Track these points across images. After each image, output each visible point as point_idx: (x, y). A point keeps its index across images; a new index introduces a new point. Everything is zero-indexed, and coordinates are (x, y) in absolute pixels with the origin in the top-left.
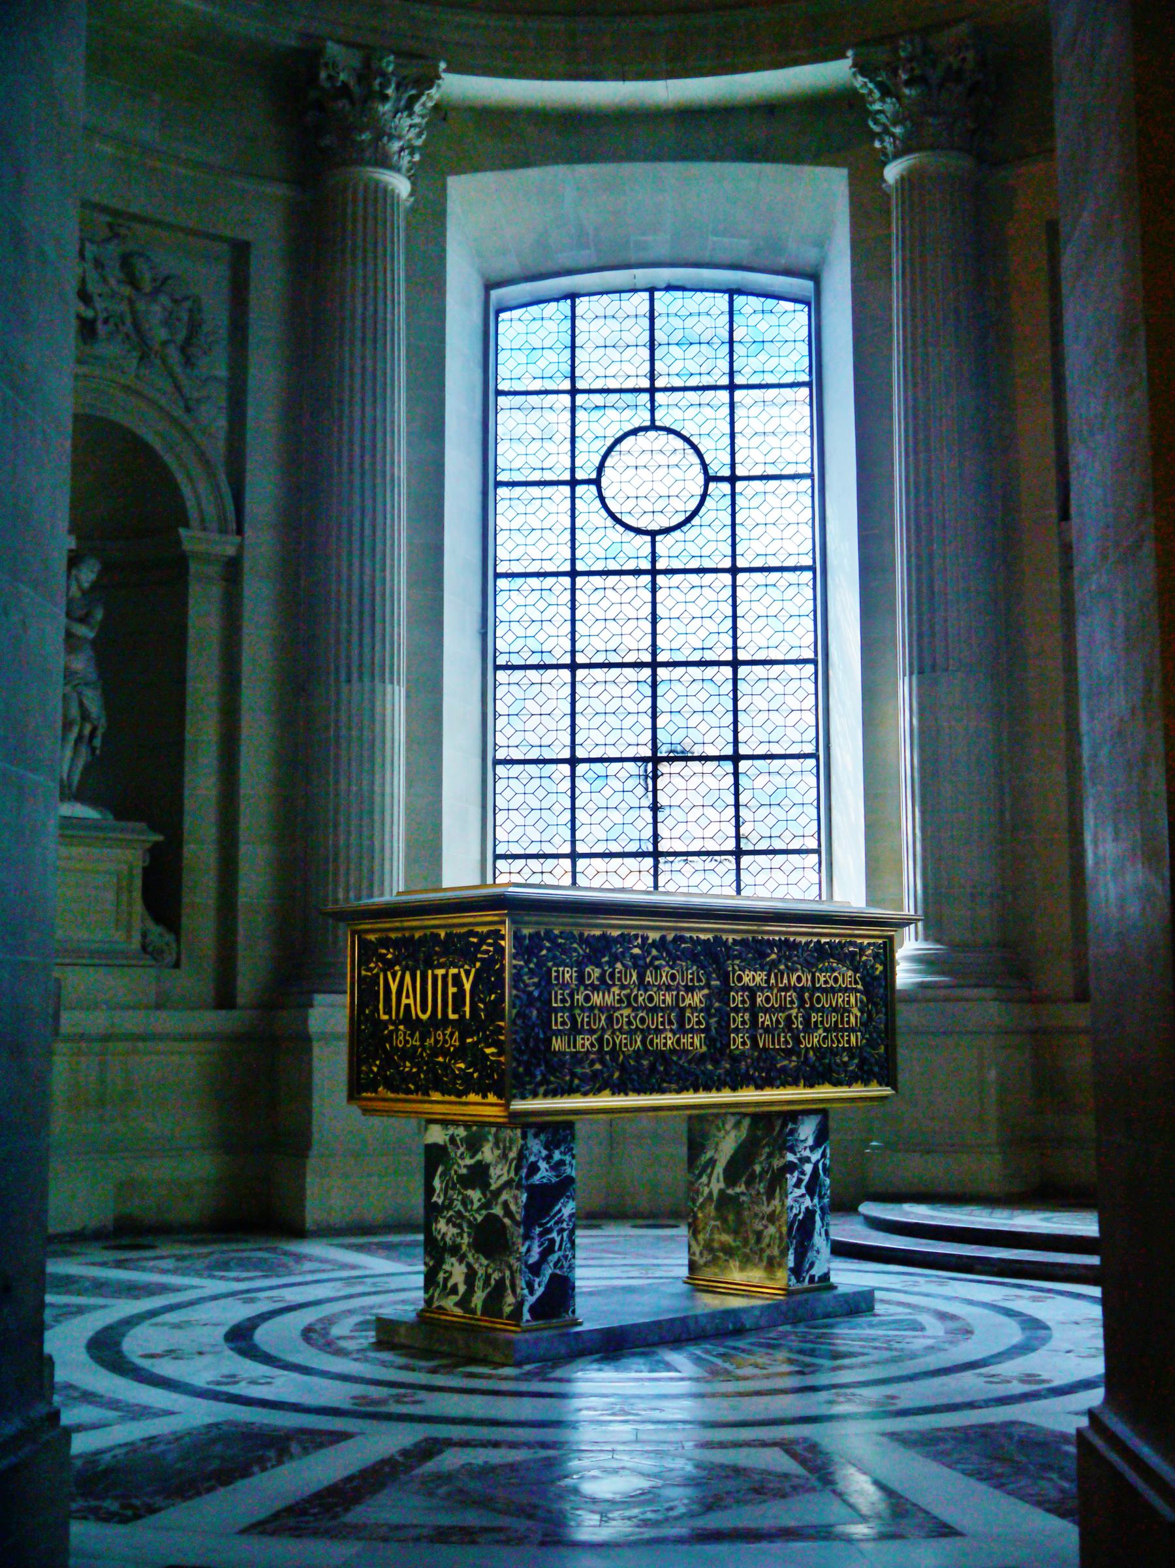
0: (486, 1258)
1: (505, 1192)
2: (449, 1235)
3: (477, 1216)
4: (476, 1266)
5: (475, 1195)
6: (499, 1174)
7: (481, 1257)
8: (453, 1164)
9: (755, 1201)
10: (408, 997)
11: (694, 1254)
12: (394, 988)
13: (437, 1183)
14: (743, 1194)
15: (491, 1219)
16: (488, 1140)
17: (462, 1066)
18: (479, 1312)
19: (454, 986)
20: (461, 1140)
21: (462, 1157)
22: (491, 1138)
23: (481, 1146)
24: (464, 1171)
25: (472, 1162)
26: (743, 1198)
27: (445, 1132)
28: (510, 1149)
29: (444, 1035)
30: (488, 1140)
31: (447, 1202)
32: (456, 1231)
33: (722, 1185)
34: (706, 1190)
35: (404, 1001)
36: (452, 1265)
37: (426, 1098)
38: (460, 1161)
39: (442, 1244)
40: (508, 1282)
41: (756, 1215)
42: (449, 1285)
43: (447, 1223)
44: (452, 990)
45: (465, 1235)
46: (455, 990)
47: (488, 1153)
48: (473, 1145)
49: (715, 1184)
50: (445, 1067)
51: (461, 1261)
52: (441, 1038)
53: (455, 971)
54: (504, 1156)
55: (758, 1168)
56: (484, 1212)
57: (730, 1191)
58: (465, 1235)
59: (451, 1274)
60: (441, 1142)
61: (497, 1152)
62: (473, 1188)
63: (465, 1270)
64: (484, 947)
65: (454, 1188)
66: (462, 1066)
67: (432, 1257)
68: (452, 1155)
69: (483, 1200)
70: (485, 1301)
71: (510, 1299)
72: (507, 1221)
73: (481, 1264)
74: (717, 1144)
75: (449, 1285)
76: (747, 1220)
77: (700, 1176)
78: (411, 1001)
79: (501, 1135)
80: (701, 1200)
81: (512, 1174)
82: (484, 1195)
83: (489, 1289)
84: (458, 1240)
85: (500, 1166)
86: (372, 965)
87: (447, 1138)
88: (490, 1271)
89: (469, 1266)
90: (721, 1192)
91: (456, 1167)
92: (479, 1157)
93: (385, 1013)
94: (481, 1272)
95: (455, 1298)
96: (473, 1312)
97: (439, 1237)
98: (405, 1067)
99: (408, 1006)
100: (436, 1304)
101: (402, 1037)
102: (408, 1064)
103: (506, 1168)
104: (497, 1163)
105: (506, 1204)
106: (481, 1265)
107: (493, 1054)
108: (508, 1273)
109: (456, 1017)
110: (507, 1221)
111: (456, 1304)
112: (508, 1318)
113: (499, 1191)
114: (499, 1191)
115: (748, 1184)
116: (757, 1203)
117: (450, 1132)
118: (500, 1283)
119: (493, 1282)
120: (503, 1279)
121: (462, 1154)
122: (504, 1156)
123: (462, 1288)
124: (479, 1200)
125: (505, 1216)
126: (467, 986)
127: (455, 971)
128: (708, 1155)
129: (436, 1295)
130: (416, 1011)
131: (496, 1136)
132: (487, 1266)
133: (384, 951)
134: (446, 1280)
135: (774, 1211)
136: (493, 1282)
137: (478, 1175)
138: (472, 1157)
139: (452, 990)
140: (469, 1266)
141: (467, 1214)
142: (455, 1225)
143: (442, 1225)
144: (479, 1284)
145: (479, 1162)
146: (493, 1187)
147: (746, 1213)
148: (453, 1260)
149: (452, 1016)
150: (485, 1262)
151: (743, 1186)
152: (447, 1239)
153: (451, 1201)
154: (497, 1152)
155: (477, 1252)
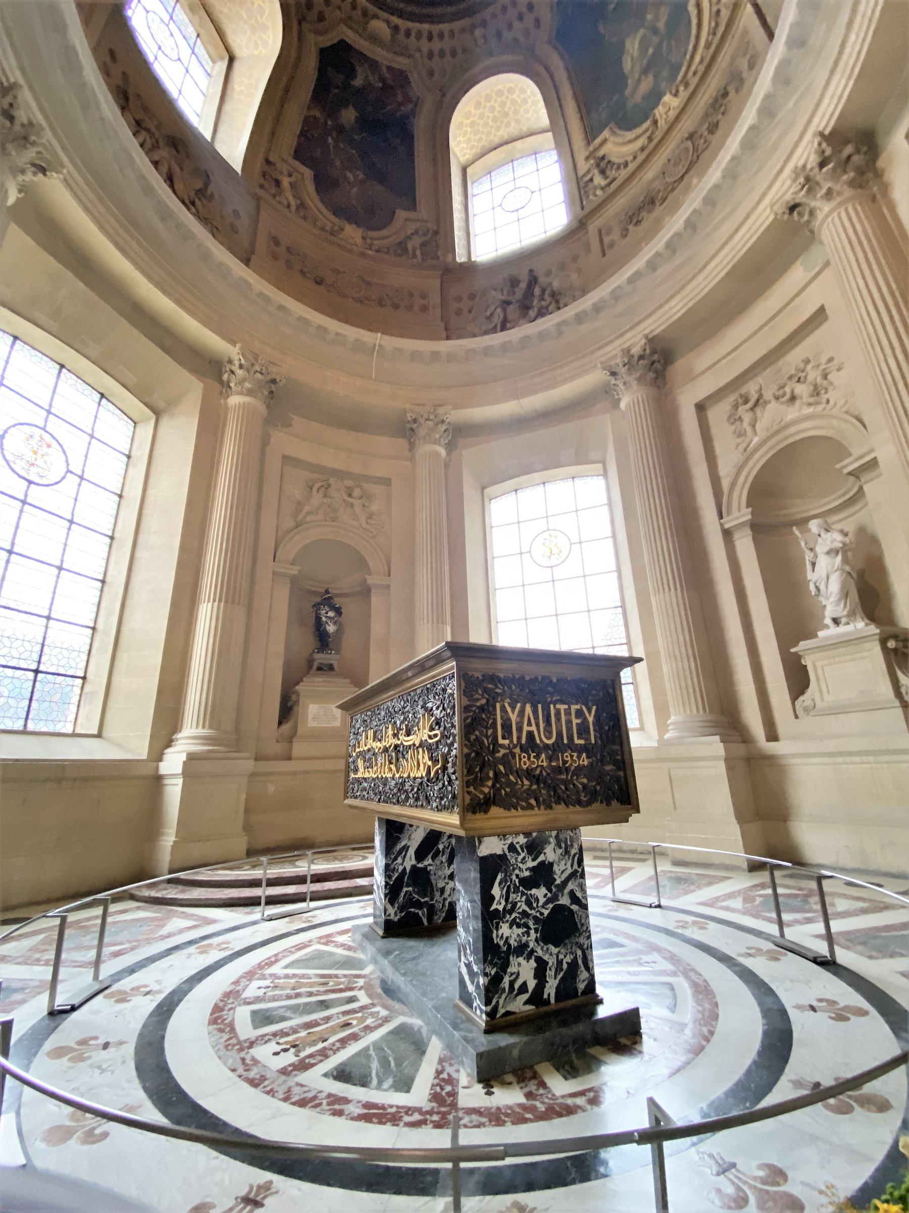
0: (556, 946)
1: (570, 883)
2: (514, 936)
3: (543, 911)
4: (546, 958)
5: (540, 893)
6: (561, 871)
7: (551, 947)
8: (514, 869)
9: (440, 868)
10: (529, 724)
11: (389, 915)
12: (514, 717)
13: (496, 891)
14: (430, 865)
15: (559, 910)
16: (550, 843)
17: (585, 781)
18: (552, 1001)
19: (577, 717)
20: (521, 847)
21: (523, 861)
22: (551, 840)
23: (543, 849)
24: (527, 874)
25: (535, 863)
26: (431, 868)
27: (502, 842)
28: (572, 846)
29: (572, 757)
30: (550, 843)
31: (509, 907)
32: (520, 931)
33: (414, 862)
34: (401, 868)
35: (526, 728)
36: (519, 964)
37: (549, 811)
38: (521, 865)
39: (505, 949)
40: (580, 962)
41: (440, 877)
42: (517, 986)
43: (511, 927)
44: (575, 721)
45: (532, 932)
46: (579, 721)
47: (550, 854)
48: (534, 848)
49: (410, 861)
50: (566, 782)
51: (528, 958)
52: (569, 758)
53: (578, 707)
54: (567, 852)
55: (441, 847)
56: (551, 906)
57: (420, 865)
58: (532, 932)
59: (518, 974)
60: (499, 852)
61: (559, 851)
62: (538, 887)
63: (535, 965)
64: (594, 692)
65: (516, 890)
66: (585, 781)
67: (495, 965)
68: (513, 861)
69: (549, 895)
70: (557, 988)
71: (584, 975)
72: (574, 907)
73: (551, 954)
74: (410, 835)
75: (517, 986)
76: (434, 882)
77: (396, 859)
78: (533, 728)
79: (562, 836)
80: (396, 875)
81: (576, 866)
82: (550, 890)
83: (562, 974)
84: (524, 939)
85: (563, 862)
86: (477, 696)
87: (507, 846)
88: (561, 957)
89: (539, 960)
90: (413, 867)
91: (517, 872)
92: (541, 858)
93: (504, 738)
94: (552, 961)
95: (525, 997)
96: (547, 1002)
97: (501, 943)
98: (523, 785)
99: (530, 735)
100: (501, 1011)
101: (525, 762)
102: (526, 782)
103: (569, 863)
104: (560, 860)
105: (572, 894)
106: (551, 954)
107: (611, 770)
108: (579, 953)
109: (582, 742)
110: (574, 907)
111: (526, 1003)
112: (584, 993)
113: (565, 883)
114: (565, 883)
115: (433, 859)
116: (440, 869)
117: (509, 842)
118: (573, 965)
119: (565, 966)
120: (575, 960)
121: (524, 858)
122: (567, 852)
123: (532, 984)
124: (545, 895)
125: (571, 904)
126: (591, 719)
127: (578, 707)
128: (403, 844)
129: (501, 1002)
130: (541, 739)
131: (557, 837)
132: (559, 952)
133: (490, 686)
134: (512, 984)
135: (453, 873)
136: (565, 966)
137: (542, 874)
138: (533, 860)
139: (575, 721)
140: (539, 960)
141: (530, 912)
142: (519, 926)
143: (505, 929)
144: (550, 973)
145: (542, 863)
146: (558, 882)
147: (432, 877)
148: (521, 959)
149: (577, 741)
150: (554, 950)
151: (430, 861)
152: (512, 942)
153: (514, 904)
154: (559, 851)
155: (546, 943)
